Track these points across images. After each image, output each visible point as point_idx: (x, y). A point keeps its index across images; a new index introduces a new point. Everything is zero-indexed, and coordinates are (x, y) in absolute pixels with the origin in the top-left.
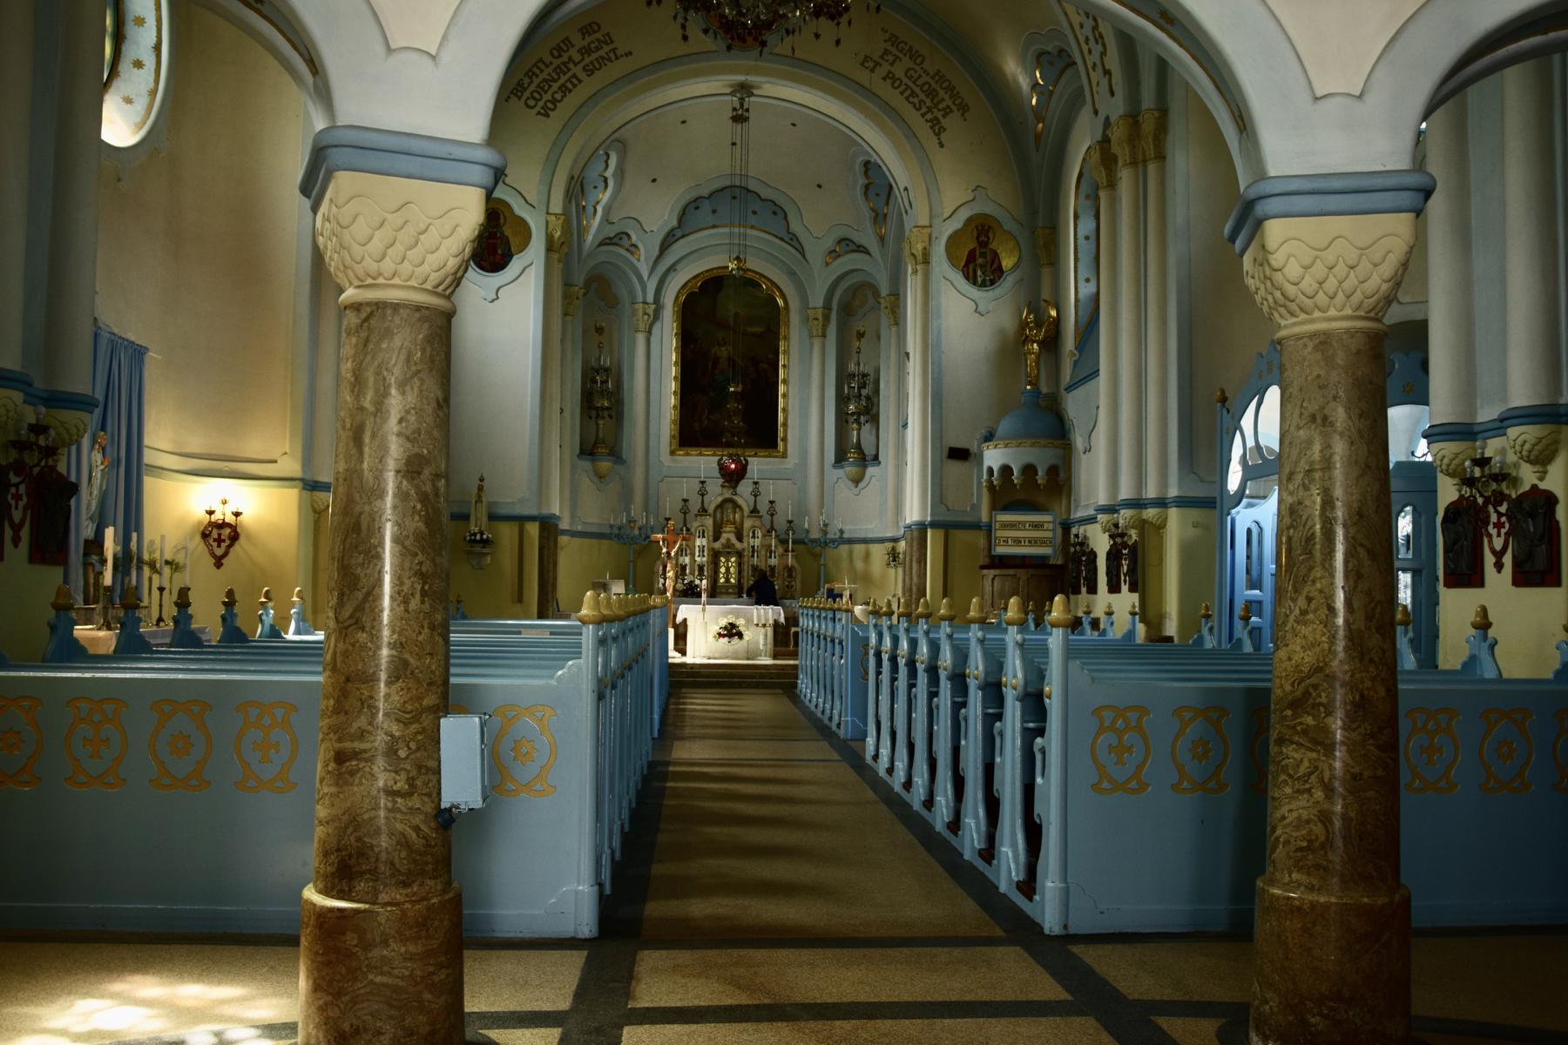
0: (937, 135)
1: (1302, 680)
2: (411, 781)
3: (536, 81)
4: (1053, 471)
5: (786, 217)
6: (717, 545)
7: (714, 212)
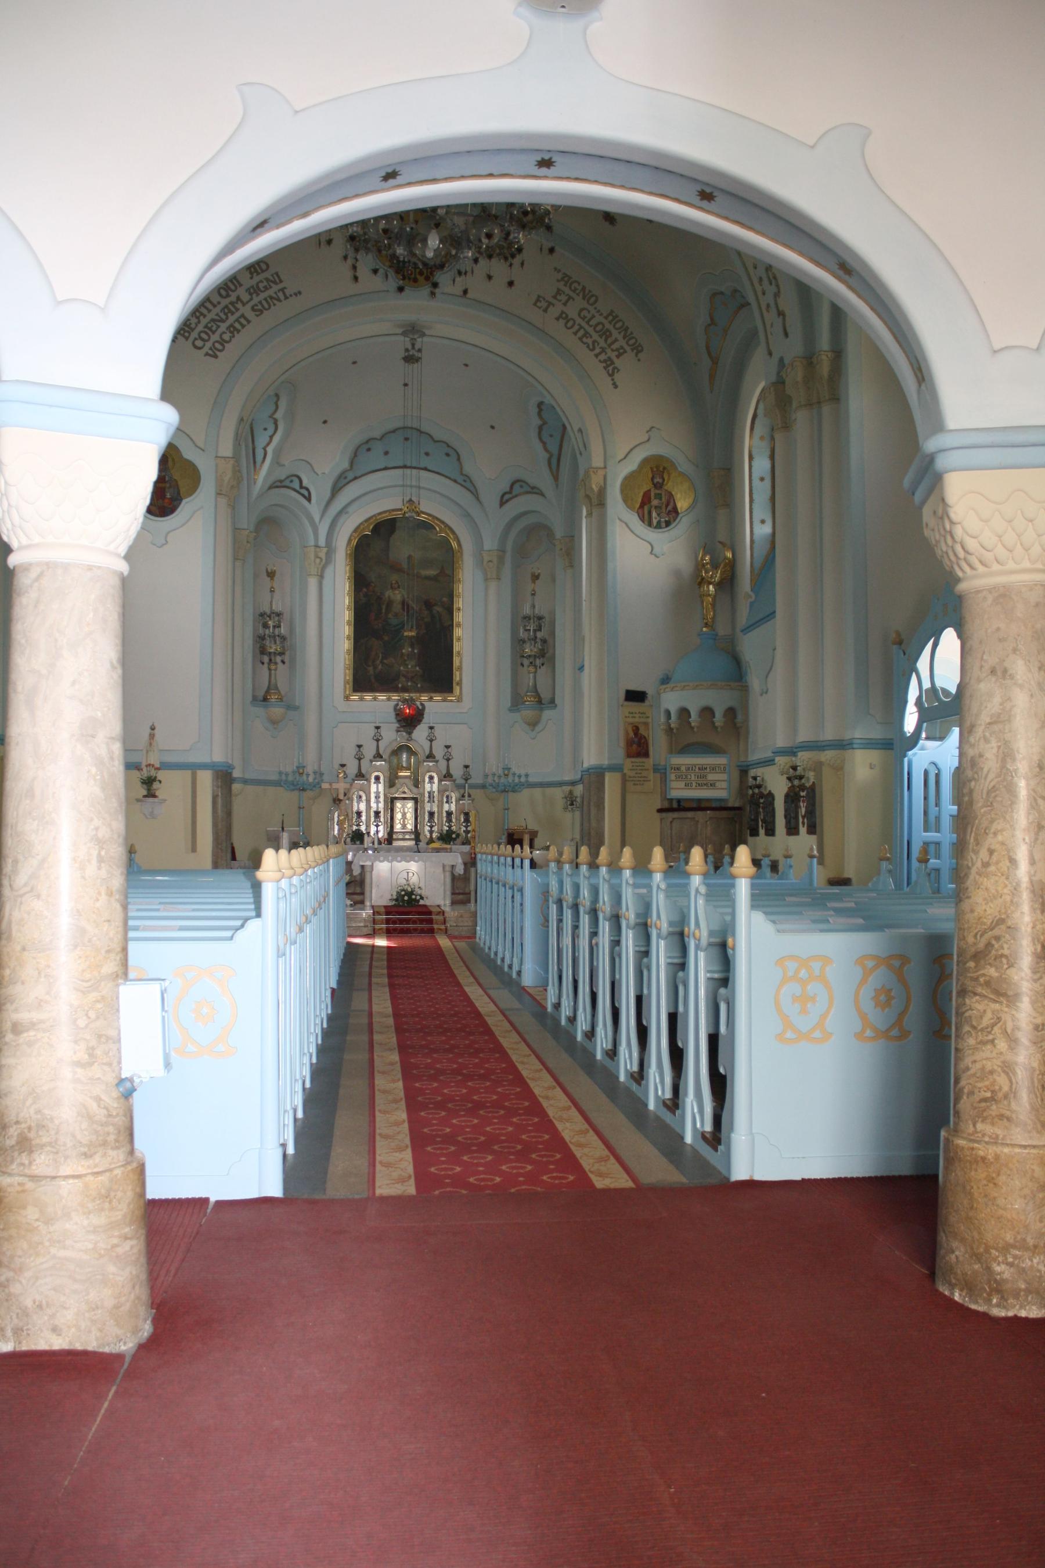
0: (611, 375)
1: (984, 932)
2: (91, 1051)
3: (204, 321)
4: (731, 712)
5: (459, 459)
7: (386, 453)
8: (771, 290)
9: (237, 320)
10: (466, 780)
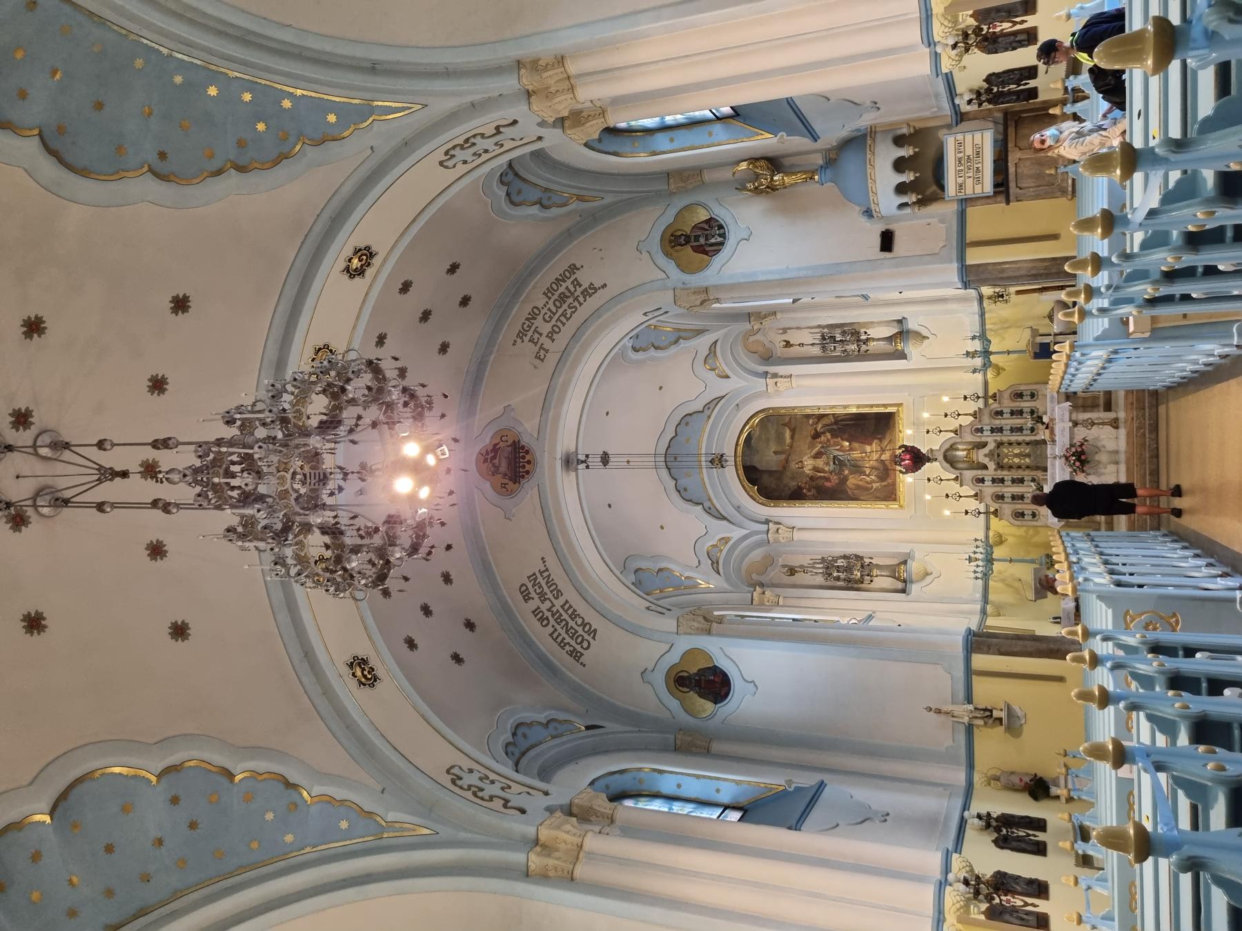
0: (596, 290)
3: (568, 640)
4: (899, 141)
6: (991, 466)
8: (481, 144)
9: (566, 611)
10: (978, 397)
